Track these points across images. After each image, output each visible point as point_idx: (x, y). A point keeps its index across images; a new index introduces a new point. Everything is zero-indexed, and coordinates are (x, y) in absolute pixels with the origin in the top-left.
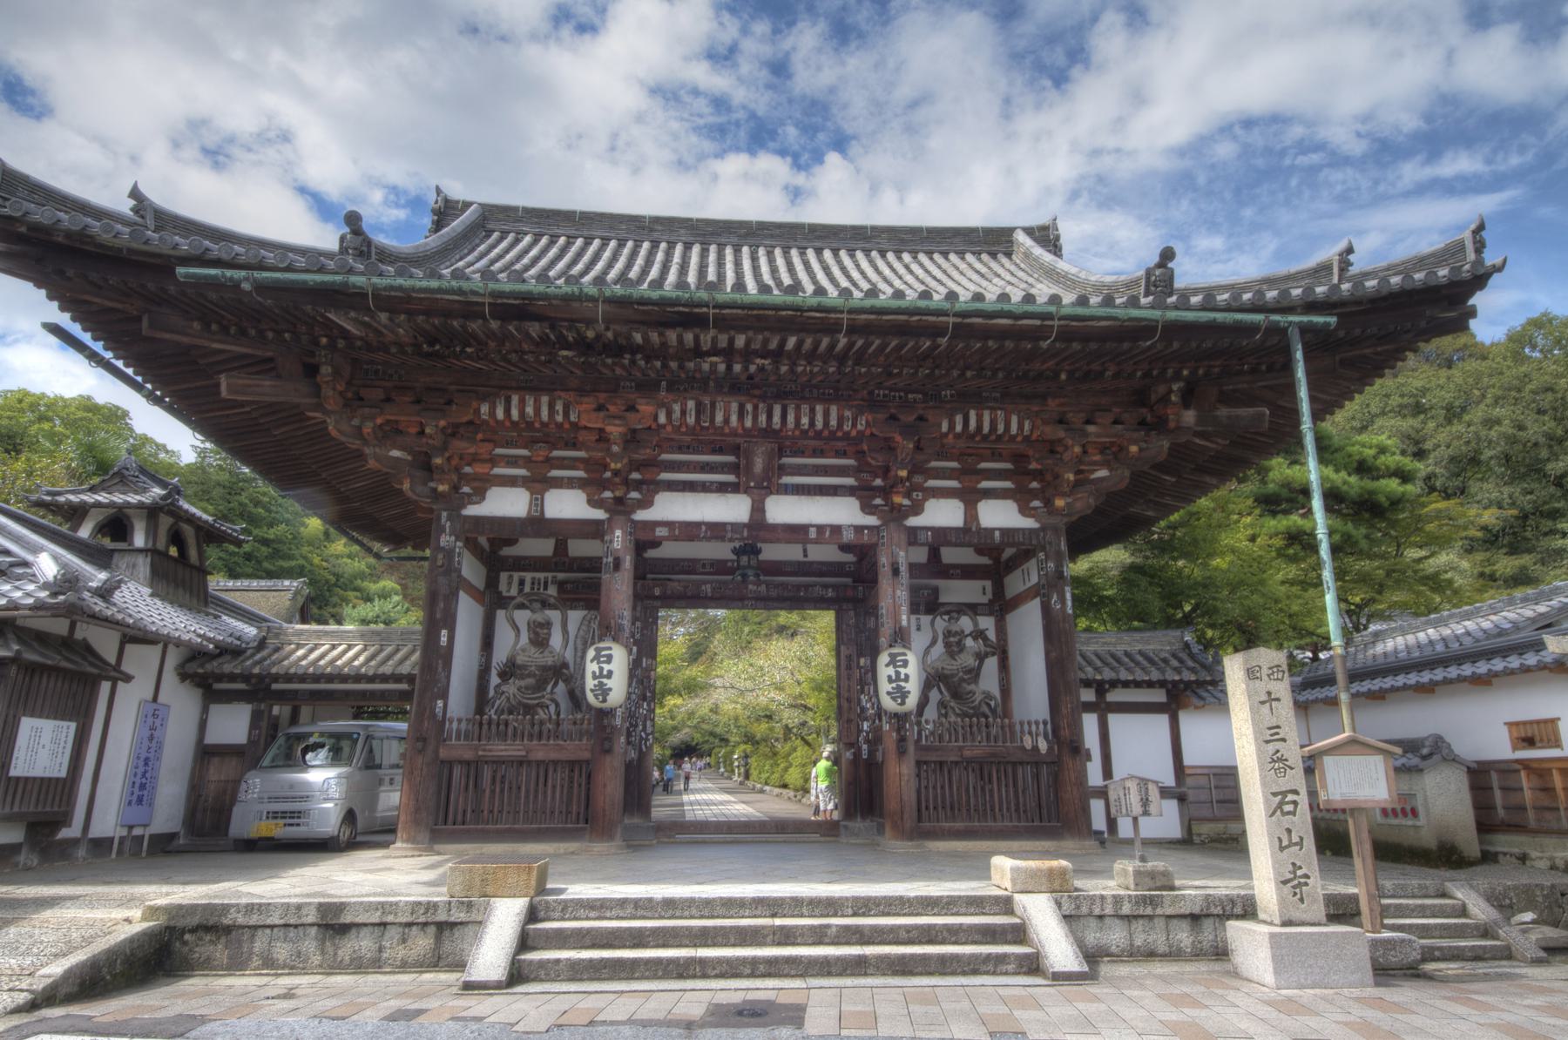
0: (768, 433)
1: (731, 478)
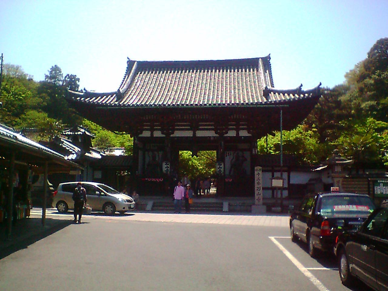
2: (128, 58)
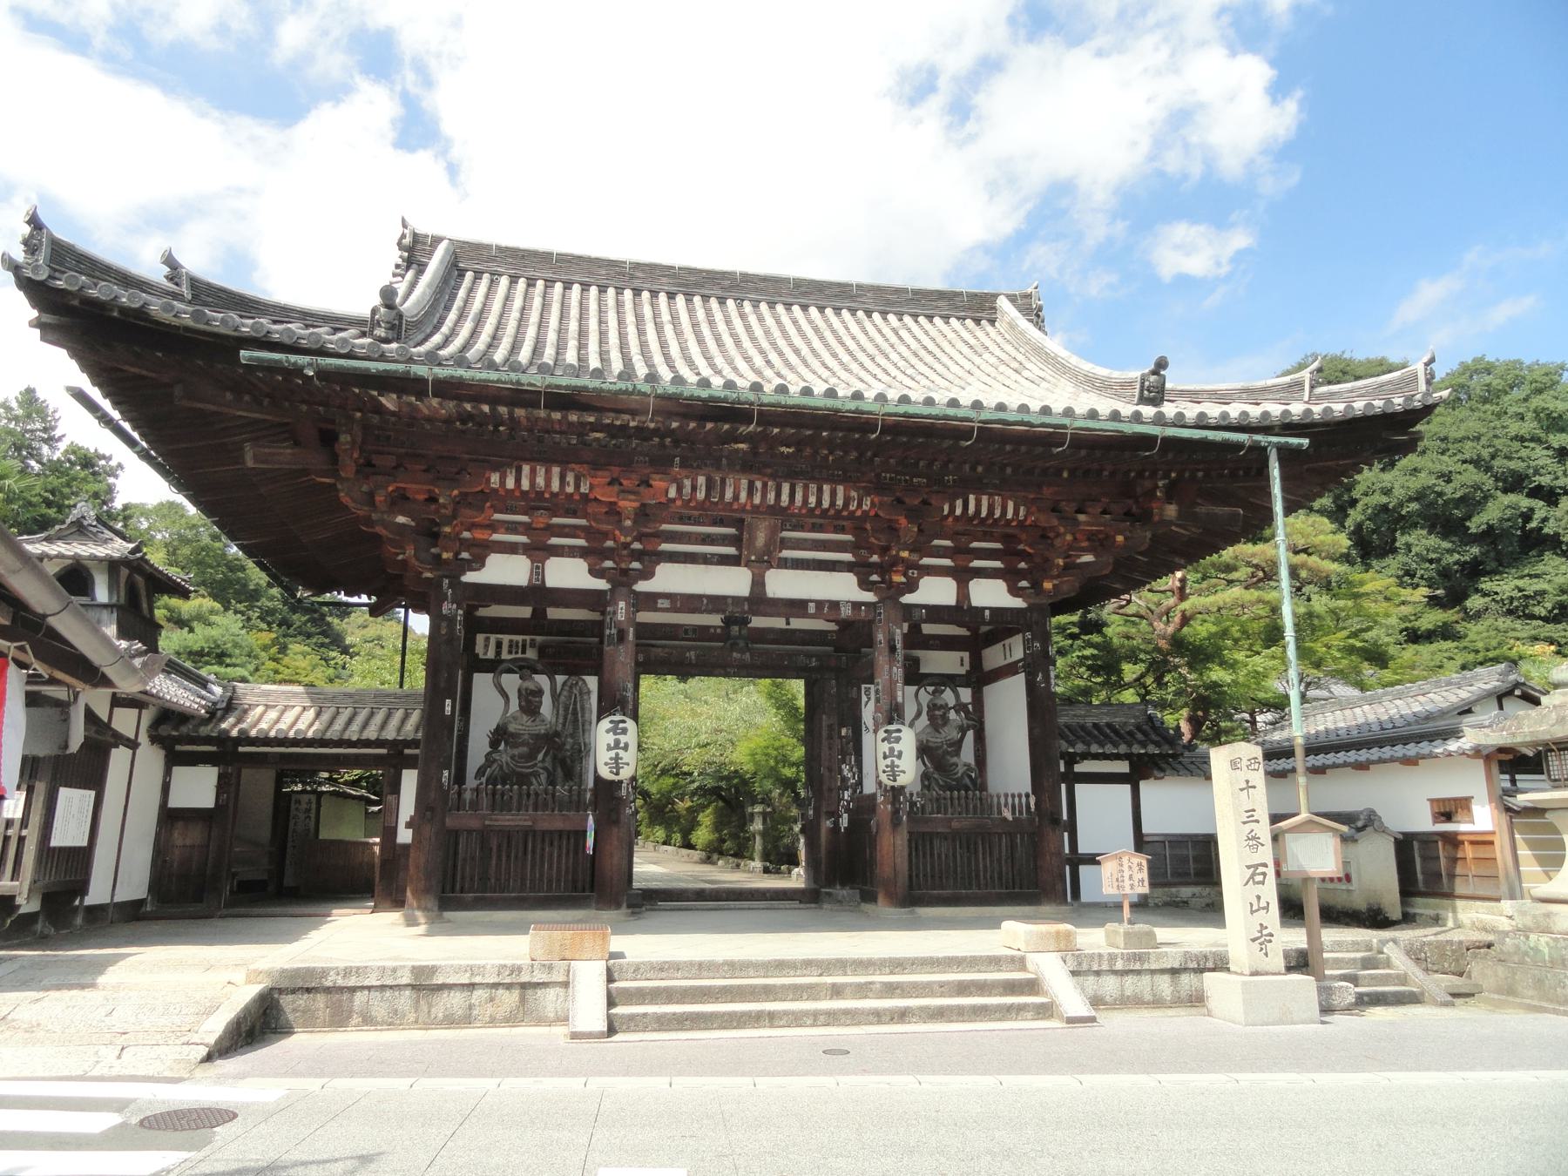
0: (775, 510)
1: (731, 550)
2: (405, 226)
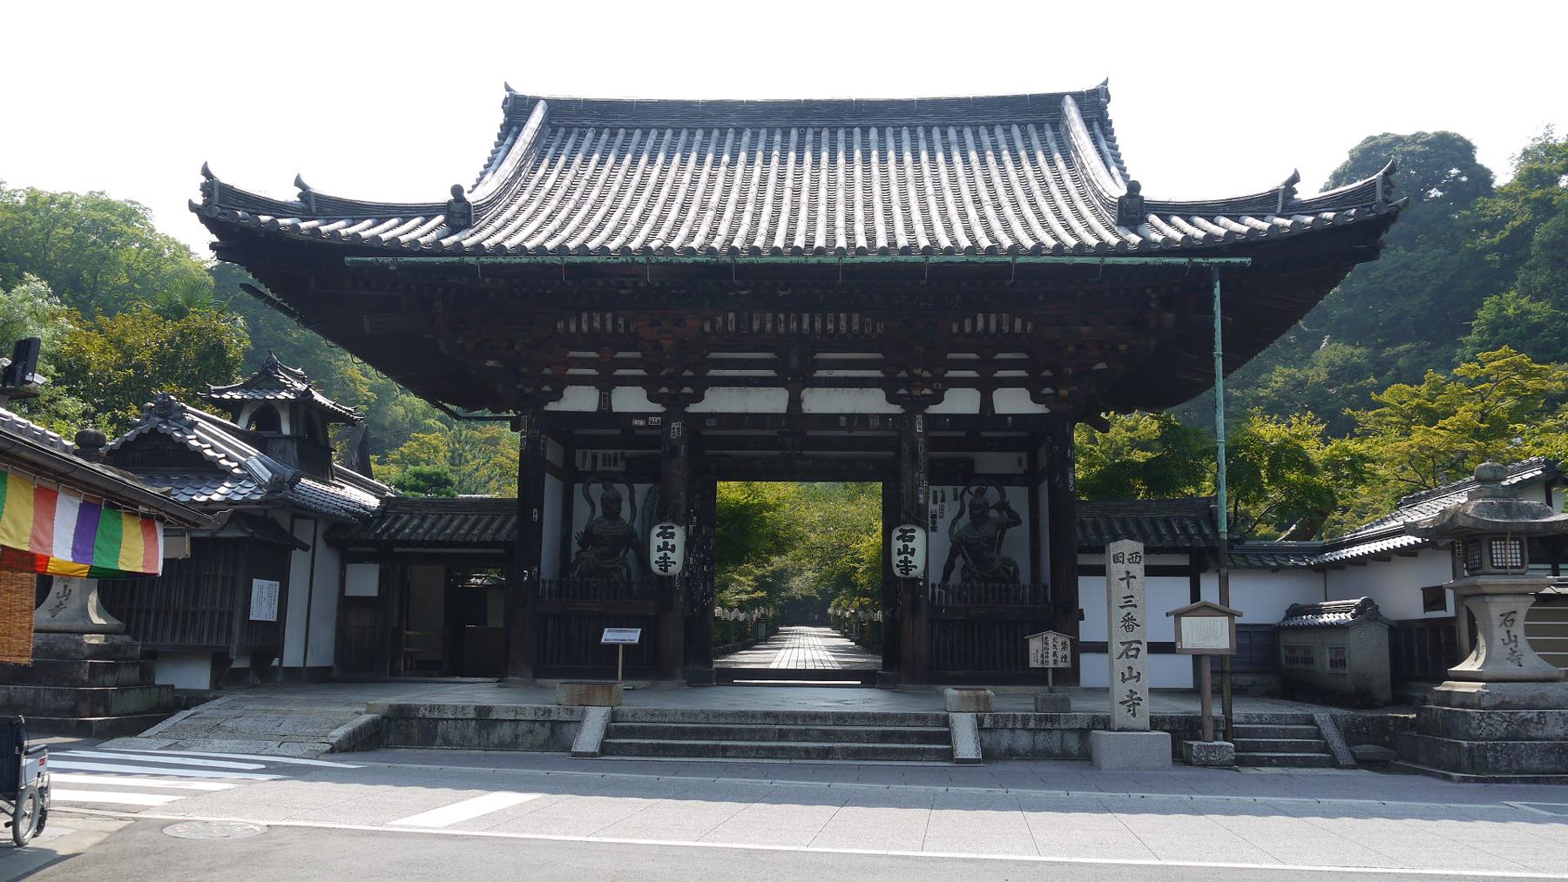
1: (771, 373)
2: (508, 88)
